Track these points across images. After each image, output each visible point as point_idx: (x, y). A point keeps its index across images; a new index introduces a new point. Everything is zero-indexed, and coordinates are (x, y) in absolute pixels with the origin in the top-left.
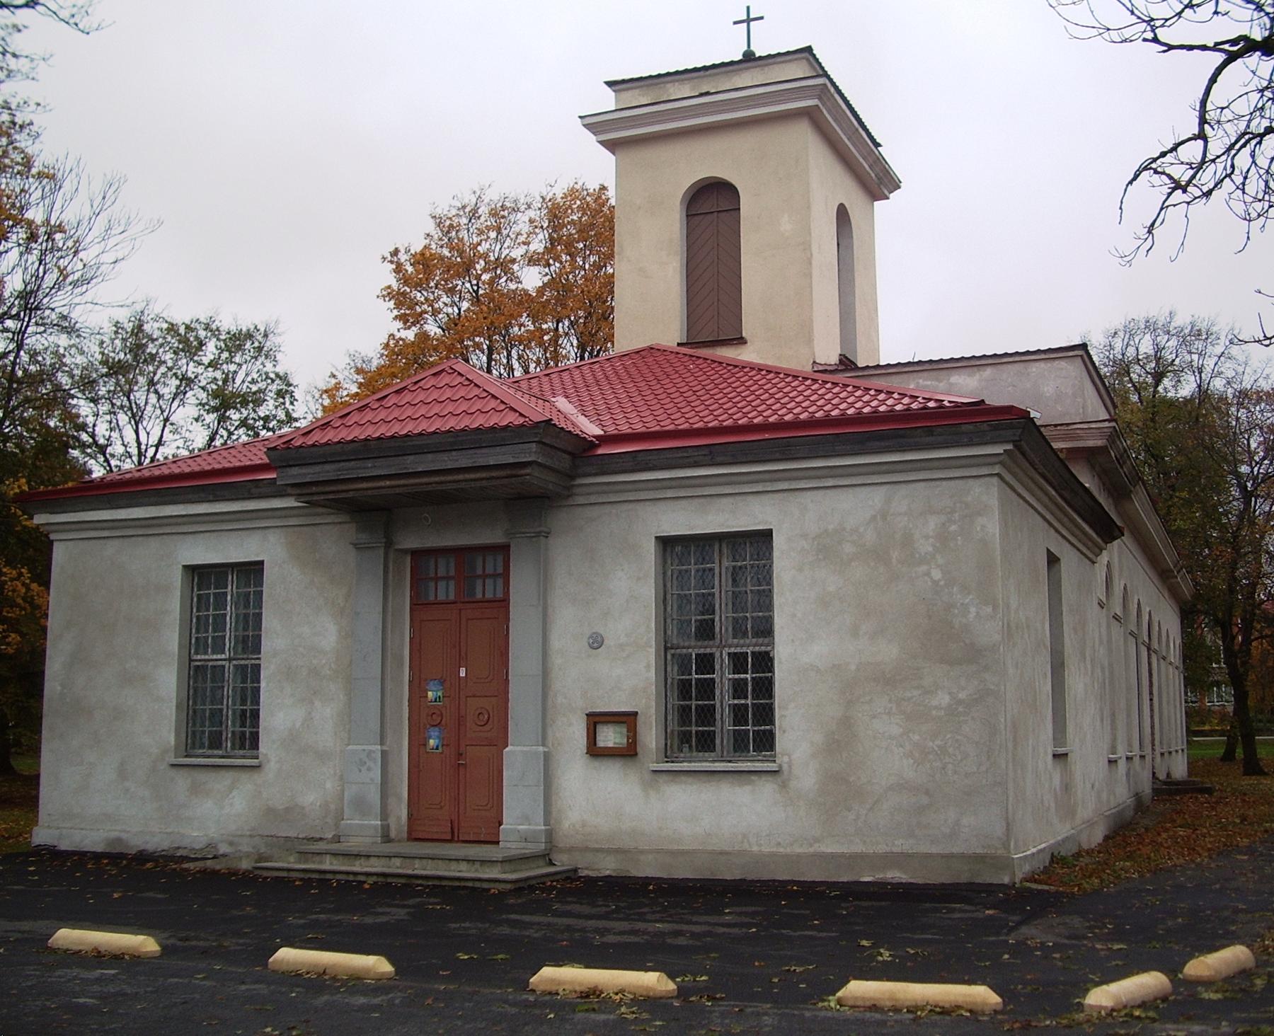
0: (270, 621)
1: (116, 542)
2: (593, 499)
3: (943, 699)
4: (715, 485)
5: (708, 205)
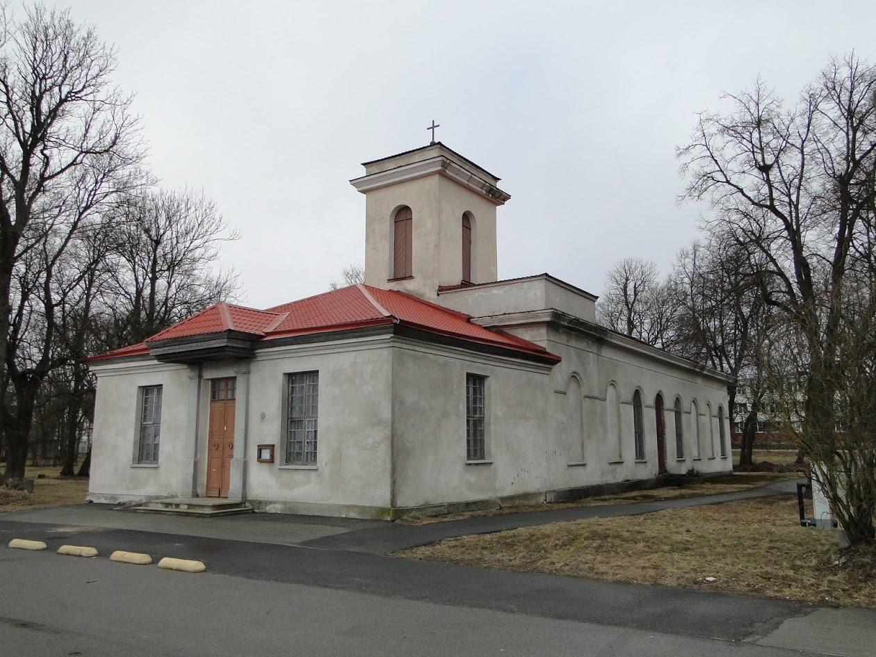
0: (164, 408)
1: (117, 377)
2: (263, 358)
3: (370, 440)
4: (301, 352)
5: (403, 216)
